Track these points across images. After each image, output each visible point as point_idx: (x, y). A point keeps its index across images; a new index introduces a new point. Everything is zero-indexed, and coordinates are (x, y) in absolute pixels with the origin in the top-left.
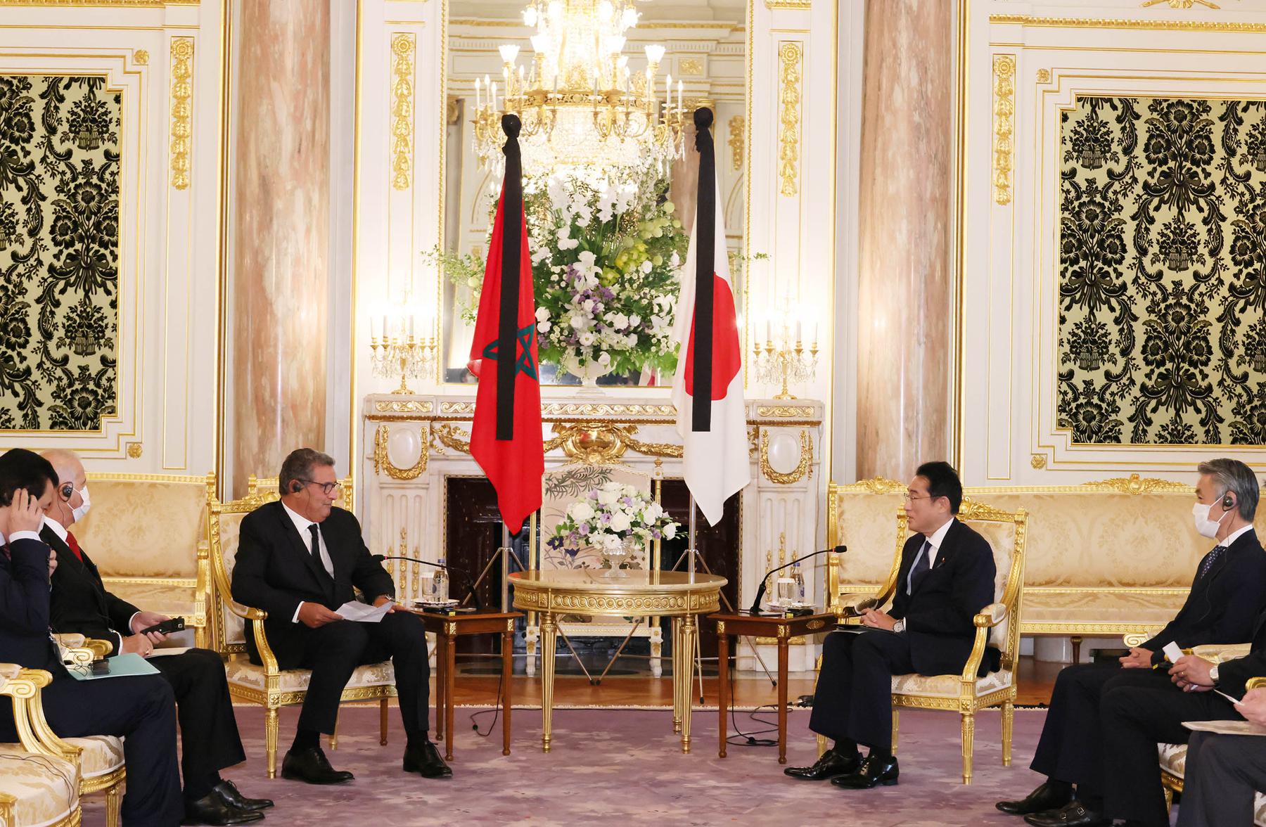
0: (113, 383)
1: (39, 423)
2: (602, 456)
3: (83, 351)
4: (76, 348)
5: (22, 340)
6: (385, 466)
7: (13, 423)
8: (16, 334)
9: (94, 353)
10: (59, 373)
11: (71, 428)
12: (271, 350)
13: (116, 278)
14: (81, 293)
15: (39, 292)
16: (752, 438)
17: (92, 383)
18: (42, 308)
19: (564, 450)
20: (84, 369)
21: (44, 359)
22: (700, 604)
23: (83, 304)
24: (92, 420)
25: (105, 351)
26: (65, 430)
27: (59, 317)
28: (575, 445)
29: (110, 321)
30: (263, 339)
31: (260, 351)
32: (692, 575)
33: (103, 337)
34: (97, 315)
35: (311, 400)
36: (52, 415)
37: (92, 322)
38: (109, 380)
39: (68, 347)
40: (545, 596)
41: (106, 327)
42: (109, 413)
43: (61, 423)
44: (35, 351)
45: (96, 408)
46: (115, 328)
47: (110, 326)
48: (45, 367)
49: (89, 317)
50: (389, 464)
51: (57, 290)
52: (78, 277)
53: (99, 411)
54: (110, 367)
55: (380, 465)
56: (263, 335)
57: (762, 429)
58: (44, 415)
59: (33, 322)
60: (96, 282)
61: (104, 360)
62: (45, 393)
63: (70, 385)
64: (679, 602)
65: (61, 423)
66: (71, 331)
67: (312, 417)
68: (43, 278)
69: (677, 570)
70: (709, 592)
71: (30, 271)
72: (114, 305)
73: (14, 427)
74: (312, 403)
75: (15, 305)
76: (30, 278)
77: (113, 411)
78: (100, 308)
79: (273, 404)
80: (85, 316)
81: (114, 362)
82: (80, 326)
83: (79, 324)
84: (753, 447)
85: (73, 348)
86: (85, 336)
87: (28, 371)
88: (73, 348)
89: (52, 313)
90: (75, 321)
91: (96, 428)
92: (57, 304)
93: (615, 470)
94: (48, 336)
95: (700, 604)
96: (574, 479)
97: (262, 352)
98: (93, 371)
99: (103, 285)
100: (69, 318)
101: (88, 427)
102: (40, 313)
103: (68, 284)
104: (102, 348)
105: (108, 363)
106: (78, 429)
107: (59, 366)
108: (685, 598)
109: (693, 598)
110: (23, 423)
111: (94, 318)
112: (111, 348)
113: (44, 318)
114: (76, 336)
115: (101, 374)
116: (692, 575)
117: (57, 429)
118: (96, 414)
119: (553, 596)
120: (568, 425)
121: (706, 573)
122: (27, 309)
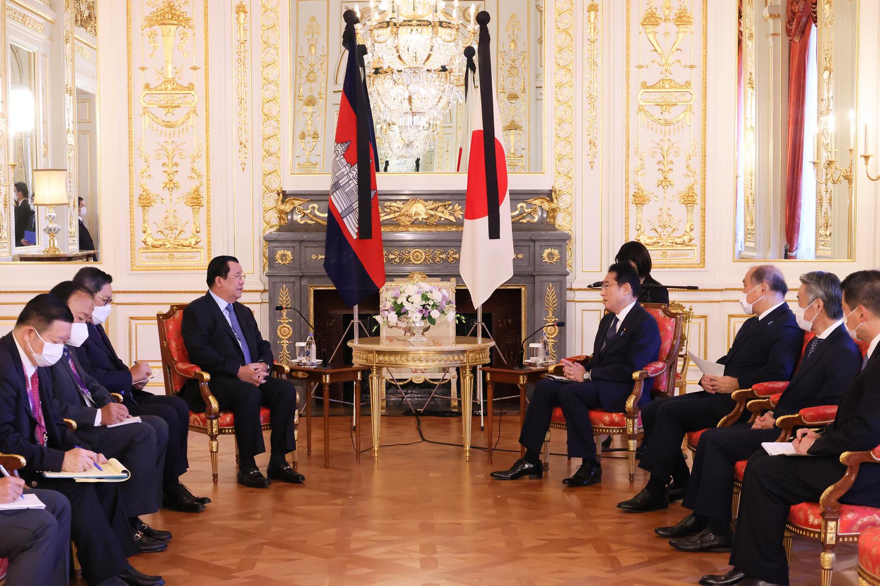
22: (476, 359)
32: (480, 339)
40: (371, 355)
64: (461, 357)
69: (470, 336)
70: (482, 350)
95: (476, 359)
108: (465, 355)
109: (471, 355)
116: (480, 339)
119: (377, 355)
121: (490, 338)
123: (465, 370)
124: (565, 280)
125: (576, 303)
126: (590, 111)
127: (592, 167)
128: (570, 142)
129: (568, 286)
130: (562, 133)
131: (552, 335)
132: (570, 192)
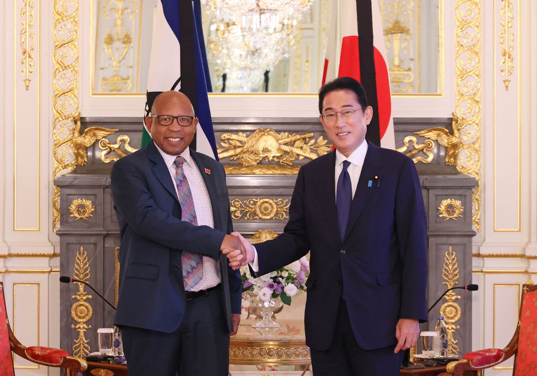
124: (470, 242)
125: (487, 275)
126: (502, 11)
127: (507, 87)
128: (476, 53)
129: (474, 251)
130: (465, 41)
131: (452, 318)
132: (477, 122)
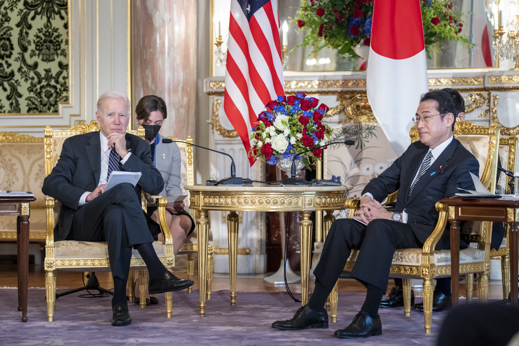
0: (67, 80)
1: (20, 109)
2: (368, 116)
3: (47, 59)
4: (43, 57)
5: (8, 53)
6: (218, 128)
7: (4, 109)
8: (4, 49)
9: (54, 60)
10: (32, 74)
11: (41, 112)
12: (151, 50)
13: (67, 8)
14: (45, 19)
15: (18, 19)
16: (487, 101)
17: (53, 80)
18: (21, 30)
19: (345, 114)
20: (48, 71)
21: (22, 65)
23: (46, 26)
24: (53, 106)
25: (61, 58)
26: (37, 113)
27: (31, 37)
28: (353, 109)
29: (63, 37)
30: (146, 43)
31: (144, 51)
33: (60, 49)
34: (56, 34)
35: (181, 85)
36: (28, 103)
37: (52, 39)
38: (64, 78)
39: (37, 57)
41: (62, 42)
42: (65, 101)
43: (34, 108)
44: (16, 60)
45: (56, 97)
46: (67, 42)
47: (64, 41)
48: (23, 70)
49: (50, 35)
50: (220, 126)
51: (29, 17)
52: (43, 8)
53: (58, 99)
54: (65, 69)
55: (215, 128)
56: (146, 39)
57: (493, 93)
58: (23, 103)
59: (15, 39)
60: (54, 11)
61: (60, 65)
62: (23, 88)
63: (40, 82)
65: (34, 108)
66: (39, 45)
67: (182, 98)
68: (20, 10)
71: (12, 5)
72: (66, 26)
73: (4, 112)
74: (183, 88)
75: (3, 29)
76: (12, 10)
77: (67, 99)
78: (57, 29)
79: (153, 88)
80: (48, 35)
81: (67, 66)
82: (45, 41)
83: (45, 40)
84: (488, 108)
85: (41, 57)
86: (48, 48)
87: (12, 74)
88: (41, 57)
89: (27, 33)
90: (41, 39)
91: (56, 111)
92: (30, 27)
93: (377, 127)
94: (24, 49)
96: (348, 134)
97: (146, 52)
98: (54, 73)
99: (59, 13)
100: (38, 37)
101: (51, 111)
102: (19, 34)
103: (36, 13)
104: (59, 56)
105: (63, 67)
106: (45, 112)
107: (32, 69)
110: (10, 109)
111: (54, 36)
112: (65, 56)
113: (22, 36)
114: (42, 49)
115: (59, 74)
117: (32, 112)
118: (56, 102)
120: (348, 96)
122: (11, 31)
123: (303, 217)
